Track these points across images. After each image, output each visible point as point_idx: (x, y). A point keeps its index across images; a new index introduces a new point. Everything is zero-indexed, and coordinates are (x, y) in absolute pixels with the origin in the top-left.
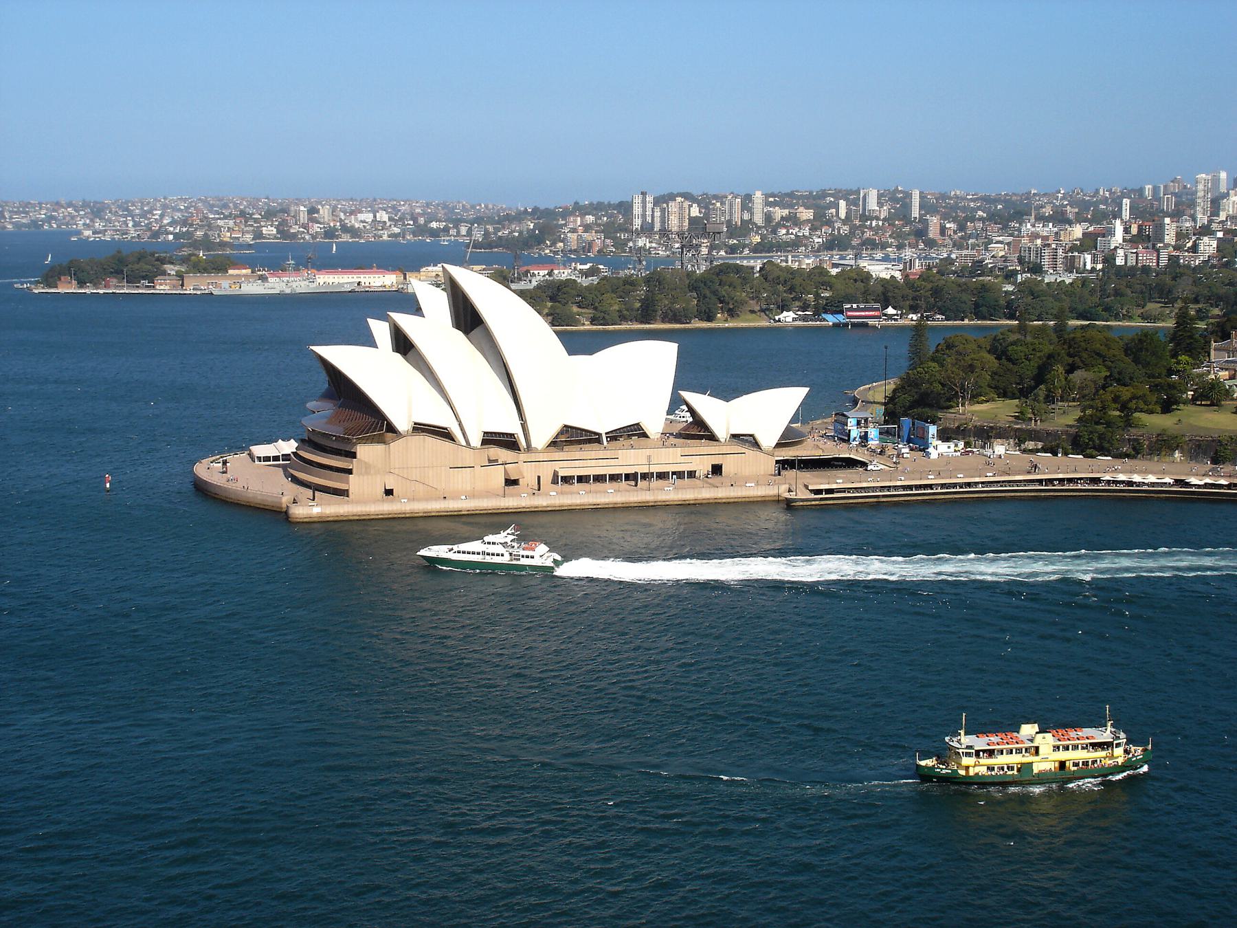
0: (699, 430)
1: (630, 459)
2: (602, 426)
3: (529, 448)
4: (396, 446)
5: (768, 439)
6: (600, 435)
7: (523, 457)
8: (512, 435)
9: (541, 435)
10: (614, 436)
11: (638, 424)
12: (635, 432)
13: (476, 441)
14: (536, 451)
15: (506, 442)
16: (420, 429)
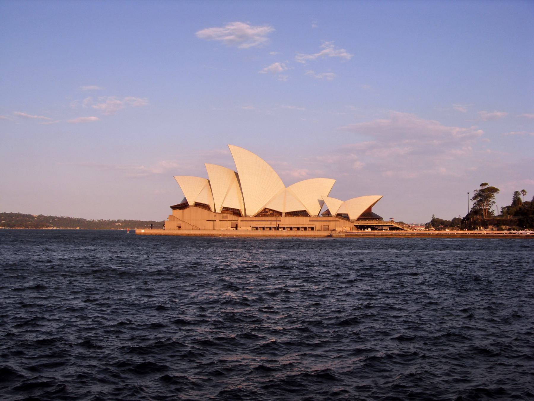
0: (328, 213)
1: (286, 222)
2: (283, 210)
3: (246, 216)
4: (186, 210)
5: (354, 215)
6: (282, 213)
7: (240, 219)
8: (238, 210)
9: (252, 210)
10: (288, 214)
11: (305, 211)
12: (304, 214)
13: (219, 210)
14: (249, 217)
15: (236, 213)
16: (197, 205)
